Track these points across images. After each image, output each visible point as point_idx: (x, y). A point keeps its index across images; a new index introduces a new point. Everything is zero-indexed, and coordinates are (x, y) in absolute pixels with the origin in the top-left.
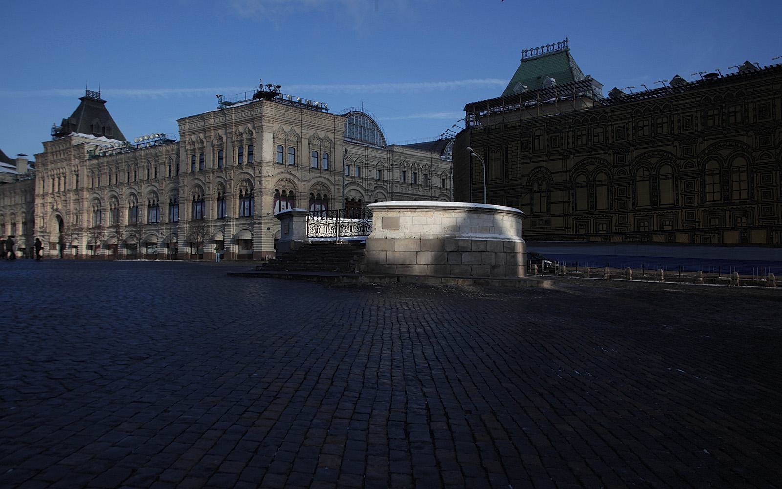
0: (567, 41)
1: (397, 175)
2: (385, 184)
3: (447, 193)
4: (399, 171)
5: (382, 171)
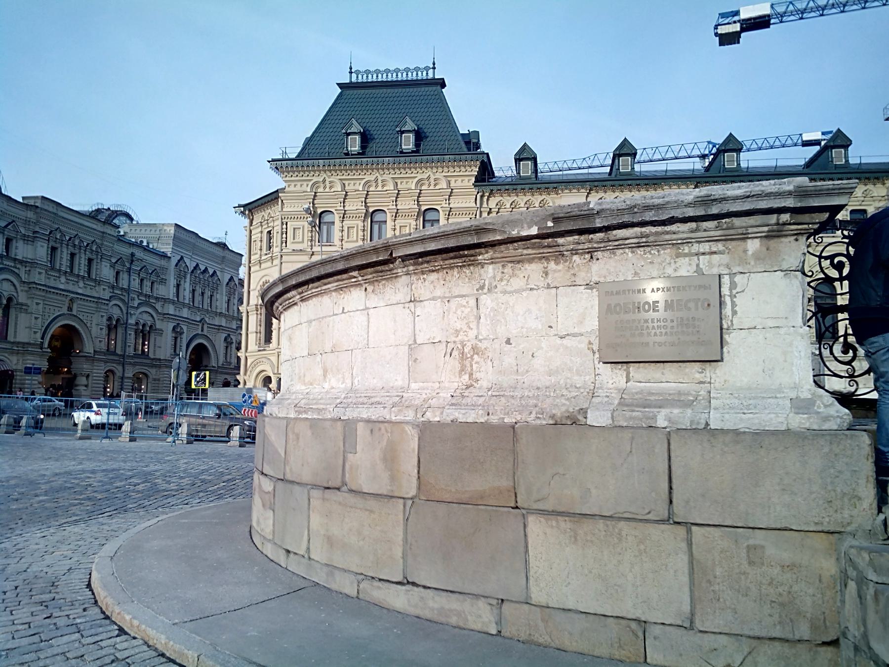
0: (434, 68)
1: (41, 251)
2: (18, 266)
3: (122, 295)
4: (46, 245)
5: (14, 241)
